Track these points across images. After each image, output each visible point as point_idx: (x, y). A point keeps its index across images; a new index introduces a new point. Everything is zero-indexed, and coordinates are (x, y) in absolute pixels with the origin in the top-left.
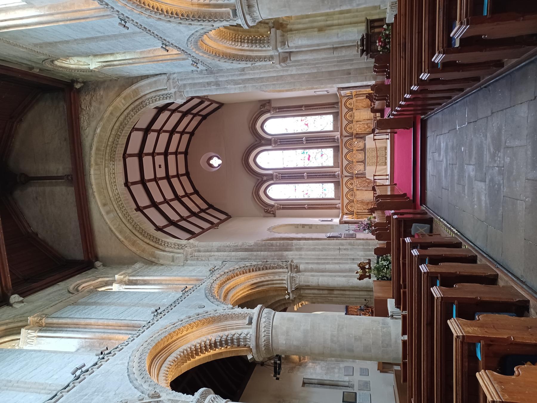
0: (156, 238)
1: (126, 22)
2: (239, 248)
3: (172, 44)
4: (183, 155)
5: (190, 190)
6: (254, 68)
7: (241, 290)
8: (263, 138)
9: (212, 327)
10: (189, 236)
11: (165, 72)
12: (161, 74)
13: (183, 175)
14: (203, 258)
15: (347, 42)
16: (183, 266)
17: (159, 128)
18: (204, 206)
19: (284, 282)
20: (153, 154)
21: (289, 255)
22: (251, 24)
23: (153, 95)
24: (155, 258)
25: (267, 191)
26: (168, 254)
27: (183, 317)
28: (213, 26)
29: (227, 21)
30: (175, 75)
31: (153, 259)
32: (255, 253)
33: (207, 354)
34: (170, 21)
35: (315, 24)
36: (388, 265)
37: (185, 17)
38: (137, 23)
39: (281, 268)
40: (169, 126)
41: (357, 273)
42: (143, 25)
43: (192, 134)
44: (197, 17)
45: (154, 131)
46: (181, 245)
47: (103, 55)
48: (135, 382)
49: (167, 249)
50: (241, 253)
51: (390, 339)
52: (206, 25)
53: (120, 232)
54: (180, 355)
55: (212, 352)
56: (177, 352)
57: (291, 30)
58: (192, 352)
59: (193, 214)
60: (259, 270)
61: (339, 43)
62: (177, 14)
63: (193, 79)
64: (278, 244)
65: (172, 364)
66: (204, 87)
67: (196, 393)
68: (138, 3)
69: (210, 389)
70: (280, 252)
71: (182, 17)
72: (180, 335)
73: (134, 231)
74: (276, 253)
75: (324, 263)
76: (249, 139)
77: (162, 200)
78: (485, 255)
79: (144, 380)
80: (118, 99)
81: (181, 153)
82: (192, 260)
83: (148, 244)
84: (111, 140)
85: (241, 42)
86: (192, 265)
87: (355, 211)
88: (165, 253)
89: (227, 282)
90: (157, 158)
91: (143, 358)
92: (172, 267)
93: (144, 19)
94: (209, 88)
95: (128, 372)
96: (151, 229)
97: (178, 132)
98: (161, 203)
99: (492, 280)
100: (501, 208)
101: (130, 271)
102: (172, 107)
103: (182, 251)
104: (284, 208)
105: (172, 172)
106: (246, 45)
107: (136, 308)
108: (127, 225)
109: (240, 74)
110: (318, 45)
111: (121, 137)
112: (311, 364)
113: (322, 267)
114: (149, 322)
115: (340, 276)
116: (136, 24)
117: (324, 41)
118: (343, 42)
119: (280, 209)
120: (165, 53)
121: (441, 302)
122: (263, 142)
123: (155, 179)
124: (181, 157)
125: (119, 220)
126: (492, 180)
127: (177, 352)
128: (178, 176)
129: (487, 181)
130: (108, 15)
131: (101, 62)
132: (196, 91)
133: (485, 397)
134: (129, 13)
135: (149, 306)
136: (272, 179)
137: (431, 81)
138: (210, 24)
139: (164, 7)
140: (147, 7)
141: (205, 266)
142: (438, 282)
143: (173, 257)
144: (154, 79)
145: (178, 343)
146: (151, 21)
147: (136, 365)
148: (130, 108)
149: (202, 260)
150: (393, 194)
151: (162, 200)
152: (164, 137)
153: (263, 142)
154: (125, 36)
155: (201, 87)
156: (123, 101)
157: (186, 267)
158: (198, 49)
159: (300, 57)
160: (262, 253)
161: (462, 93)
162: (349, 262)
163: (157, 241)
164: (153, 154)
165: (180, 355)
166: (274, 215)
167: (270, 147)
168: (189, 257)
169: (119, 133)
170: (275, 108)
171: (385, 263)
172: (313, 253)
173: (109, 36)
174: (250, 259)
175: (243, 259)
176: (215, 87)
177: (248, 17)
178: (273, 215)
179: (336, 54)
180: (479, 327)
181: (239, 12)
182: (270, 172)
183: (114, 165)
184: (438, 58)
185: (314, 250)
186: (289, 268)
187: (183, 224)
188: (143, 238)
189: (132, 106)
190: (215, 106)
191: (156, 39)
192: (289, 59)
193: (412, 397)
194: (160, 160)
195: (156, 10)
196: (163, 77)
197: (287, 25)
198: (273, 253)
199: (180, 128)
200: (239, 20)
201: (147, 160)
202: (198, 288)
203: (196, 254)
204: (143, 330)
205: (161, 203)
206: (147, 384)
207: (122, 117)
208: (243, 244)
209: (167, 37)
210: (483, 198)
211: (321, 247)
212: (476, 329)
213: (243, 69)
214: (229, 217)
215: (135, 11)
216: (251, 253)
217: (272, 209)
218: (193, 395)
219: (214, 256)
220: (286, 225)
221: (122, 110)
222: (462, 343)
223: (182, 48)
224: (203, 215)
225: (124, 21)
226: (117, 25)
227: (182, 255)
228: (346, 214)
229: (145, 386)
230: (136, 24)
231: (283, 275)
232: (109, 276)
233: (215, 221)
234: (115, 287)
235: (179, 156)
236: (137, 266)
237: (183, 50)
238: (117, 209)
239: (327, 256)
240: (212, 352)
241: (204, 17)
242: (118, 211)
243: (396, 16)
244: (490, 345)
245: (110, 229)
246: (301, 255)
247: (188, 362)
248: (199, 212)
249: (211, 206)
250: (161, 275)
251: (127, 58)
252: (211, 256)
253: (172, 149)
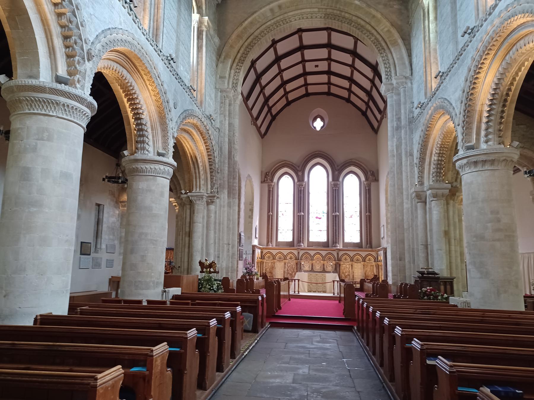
0: (244, 61)
1: (469, 34)
2: (232, 146)
3: (442, 83)
4: (326, 90)
5: (291, 97)
6: (412, 165)
7: (190, 146)
8: (340, 173)
9: (155, 116)
10: (245, 94)
11: (415, 74)
12: (412, 69)
13: (307, 89)
14: (222, 109)
15: (433, 258)
16: (216, 88)
17: (356, 66)
18: (274, 111)
19: (198, 189)
20: (329, 59)
21: (224, 195)
22: (458, 164)
23: (391, 61)
24: (225, 59)
25: (287, 176)
26: (228, 73)
27: (165, 86)
28: (459, 125)
29: (462, 140)
30: (409, 85)
31: (223, 57)
32: (227, 161)
33: (129, 110)
34: (467, 80)
35: (452, 228)
36: (213, 289)
37: (470, 97)
38: (468, 46)
39: (211, 186)
40: (357, 77)
41: (206, 260)
42: (464, 53)
43: (348, 100)
44: (469, 109)
45: (353, 61)
46: (237, 86)
47: (436, 8)
48: (103, 35)
49: (233, 71)
50: (227, 147)
51: (143, 289)
52: (459, 118)
53: (251, 23)
54: (128, 82)
55: (131, 115)
56: (131, 80)
57: (448, 204)
58: (131, 94)
59: (267, 99)
60: (210, 165)
61: (432, 251)
62: (474, 88)
63: (405, 103)
64: (235, 184)
65: (120, 74)
66: (396, 115)
67: (91, 98)
68: (488, 48)
69: (96, 112)
70: (227, 186)
71: (469, 93)
72: (148, 83)
73: (252, 37)
74: (226, 183)
75: (215, 229)
76: (340, 159)
77: (283, 67)
78: (224, 380)
79: (105, 44)
80: (388, 24)
81: (329, 88)
82: (221, 97)
83: (238, 52)
84: (347, 15)
85: (440, 153)
86: (216, 97)
87: (265, 261)
88: (229, 69)
89: (199, 133)
90: (326, 63)
91: (126, 44)
92: (214, 76)
93: (471, 53)
94: (395, 119)
95: (113, 28)
96: (253, 56)
97: (350, 86)
98: (279, 67)
99: (201, 385)
100: (268, 396)
101: (212, 32)
102: (377, 80)
103: (230, 86)
104: (269, 191)
105: (311, 79)
106: (436, 158)
107: (174, 38)
108: (259, 31)
109: (406, 152)
110: (431, 230)
111: (349, 26)
112: (117, 212)
113: (212, 227)
114: (161, 52)
115: (203, 243)
116: (466, 45)
117: (435, 237)
118: (432, 254)
119: (269, 188)
120: (434, 75)
121: (182, 337)
122: (337, 173)
123: (304, 61)
124: (325, 88)
125: (264, 21)
126: (295, 389)
127: (131, 80)
128: (306, 84)
129: (294, 385)
130: (478, 14)
131: (428, 6)
132: (392, 105)
133: (100, 372)
134: (479, 38)
135: (177, 51)
136: (299, 181)
137: (393, 337)
138: (461, 122)
139: (482, 76)
140: (484, 57)
141: (215, 110)
142: (200, 335)
143: (225, 77)
144: (407, 63)
145: (140, 81)
146: (468, 61)
147: (120, 37)
148: (378, 36)
149: (221, 107)
150: (281, 297)
151: (283, 67)
152: (346, 71)
153: (337, 173)
154: (455, 33)
155: (396, 112)
156: (386, 29)
157: (214, 90)
158: (436, 109)
159: (420, 212)
160: (227, 168)
161: (378, 366)
162: (216, 253)
163: (242, 61)
164: (329, 59)
165: (128, 82)
166: (263, 182)
167: (331, 179)
168: (225, 94)
169: (353, 24)
170: (369, 186)
171: (215, 287)
172: (226, 219)
173: (456, 15)
174: (221, 156)
175: (221, 149)
176: (395, 125)
177: (465, 161)
178: (263, 180)
179: (421, 247)
180: (161, 370)
181: (471, 153)
182: (306, 179)
183: (321, 18)
184: (416, 344)
185: (229, 219)
186: (211, 195)
187: (258, 89)
188: (244, 47)
189: (380, 39)
190: (376, 124)
191: (449, 66)
192: (419, 201)
193: (90, 307)
194: (323, 66)
195: (480, 66)
196: (409, 72)
197: (454, 200)
198: (226, 179)
199: (354, 88)
200: (462, 152)
201: (323, 53)
202: (194, 103)
203: (227, 101)
204: (153, 44)
205: (279, 67)
206: (101, 48)
207: (370, 28)
208: (236, 150)
209: (450, 78)
210: (278, 380)
211: (231, 226)
212: (159, 368)
213: (411, 155)
214: (263, 136)
215: (480, 44)
216: (227, 157)
217: (269, 180)
218: (90, 95)
219: (225, 120)
220: (253, 193)
221: (377, 28)
222: (147, 355)
223: (437, 93)
224: (266, 109)
225: (471, 32)
226: (467, 24)
227: (226, 87)
228: (262, 252)
229: (98, 46)
230: (466, 45)
231: (205, 188)
232: (207, 10)
233: (259, 122)
234: (196, 17)
235: (326, 86)
236: (217, 40)
237: (435, 94)
238: (275, 20)
239: (222, 232)
240: (131, 115)
241: (468, 117)
242: (273, 21)
243: (456, 306)
244: (144, 380)
245: (255, 12)
246: (224, 207)
247: (121, 91)
248: (268, 106)
249: (274, 118)
250: (206, 64)
251: (431, 36)
252: (225, 116)
253: (334, 80)
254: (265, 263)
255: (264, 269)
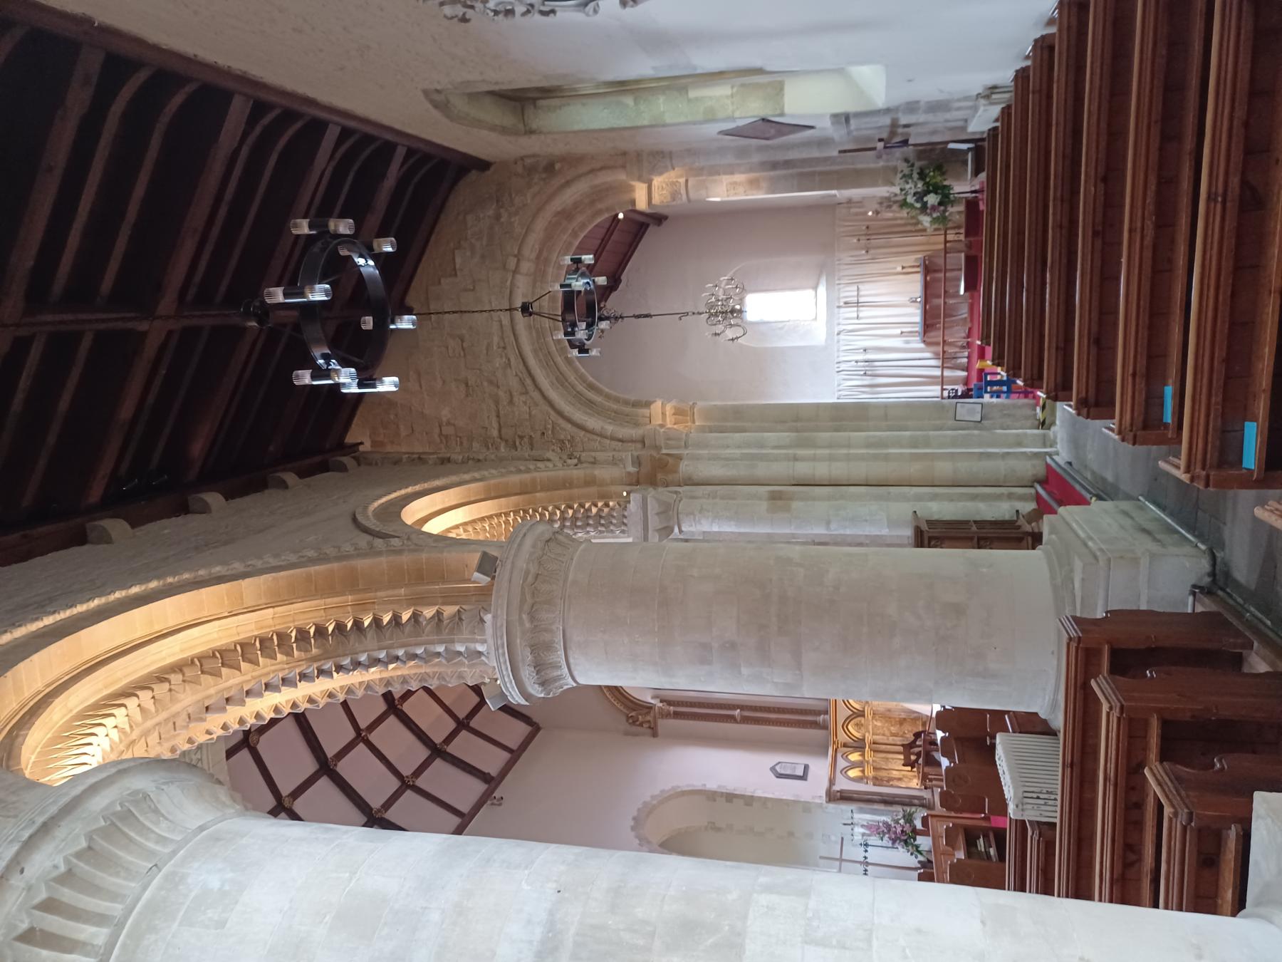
35: (762, 470)
57: (690, 482)
119: (667, 715)
178: (649, 731)
197: (679, 458)
217: (648, 718)
228: (845, 745)
254: (877, 738)
255: (891, 740)
